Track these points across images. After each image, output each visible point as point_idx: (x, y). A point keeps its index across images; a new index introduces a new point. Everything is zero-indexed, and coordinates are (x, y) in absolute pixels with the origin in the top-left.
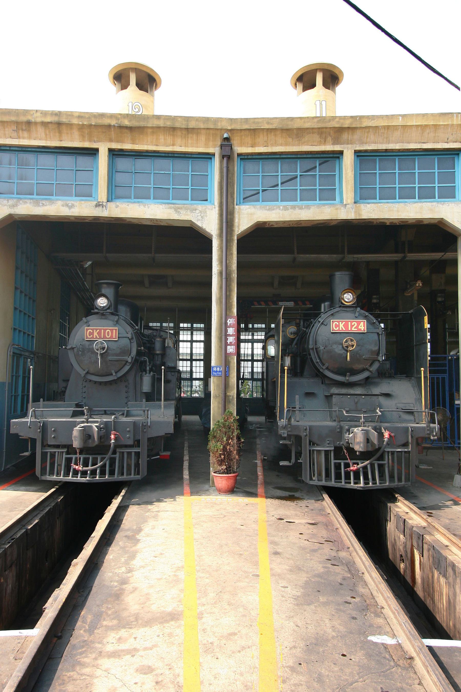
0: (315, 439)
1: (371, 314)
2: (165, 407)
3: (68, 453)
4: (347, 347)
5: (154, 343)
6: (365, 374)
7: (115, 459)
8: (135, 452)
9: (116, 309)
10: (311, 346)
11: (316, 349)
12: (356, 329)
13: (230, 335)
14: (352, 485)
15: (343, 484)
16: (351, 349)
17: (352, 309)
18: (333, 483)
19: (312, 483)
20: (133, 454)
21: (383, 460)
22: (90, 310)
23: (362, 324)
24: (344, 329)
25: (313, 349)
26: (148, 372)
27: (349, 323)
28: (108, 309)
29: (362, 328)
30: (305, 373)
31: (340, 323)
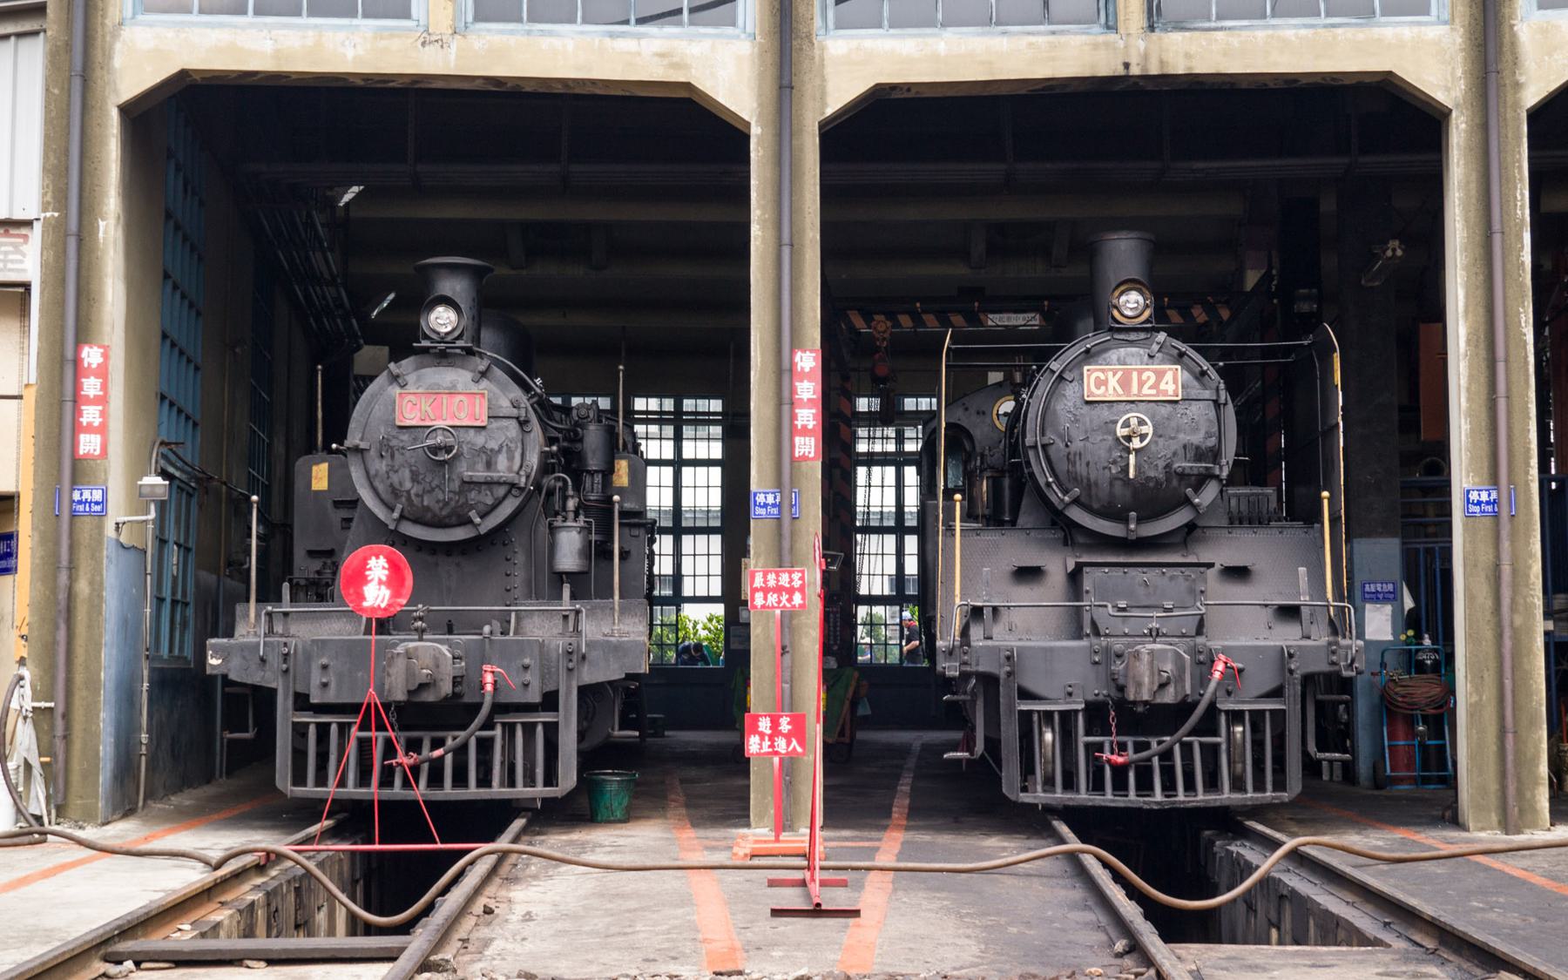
0: (1032, 685)
1: (1193, 348)
2: (623, 611)
3: (364, 727)
4: (1129, 438)
5: (581, 440)
6: (1179, 518)
7: (492, 740)
8: (544, 724)
9: (477, 339)
10: (1029, 441)
11: (1044, 447)
12: (1154, 392)
13: (802, 404)
14: (1132, 798)
15: (1108, 798)
16: (1136, 443)
17: (1142, 335)
18: (1083, 796)
19: (1025, 798)
20: (540, 729)
21: (1216, 733)
22: (405, 341)
23: (1169, 376)
24: (1120, 391)
25: (1035, 447)
26: (571, 515)
27: (1135, 375)
28: (459, 337)
29: (1170, 388)
30: (1021, 521)
31: (1110, 374)
